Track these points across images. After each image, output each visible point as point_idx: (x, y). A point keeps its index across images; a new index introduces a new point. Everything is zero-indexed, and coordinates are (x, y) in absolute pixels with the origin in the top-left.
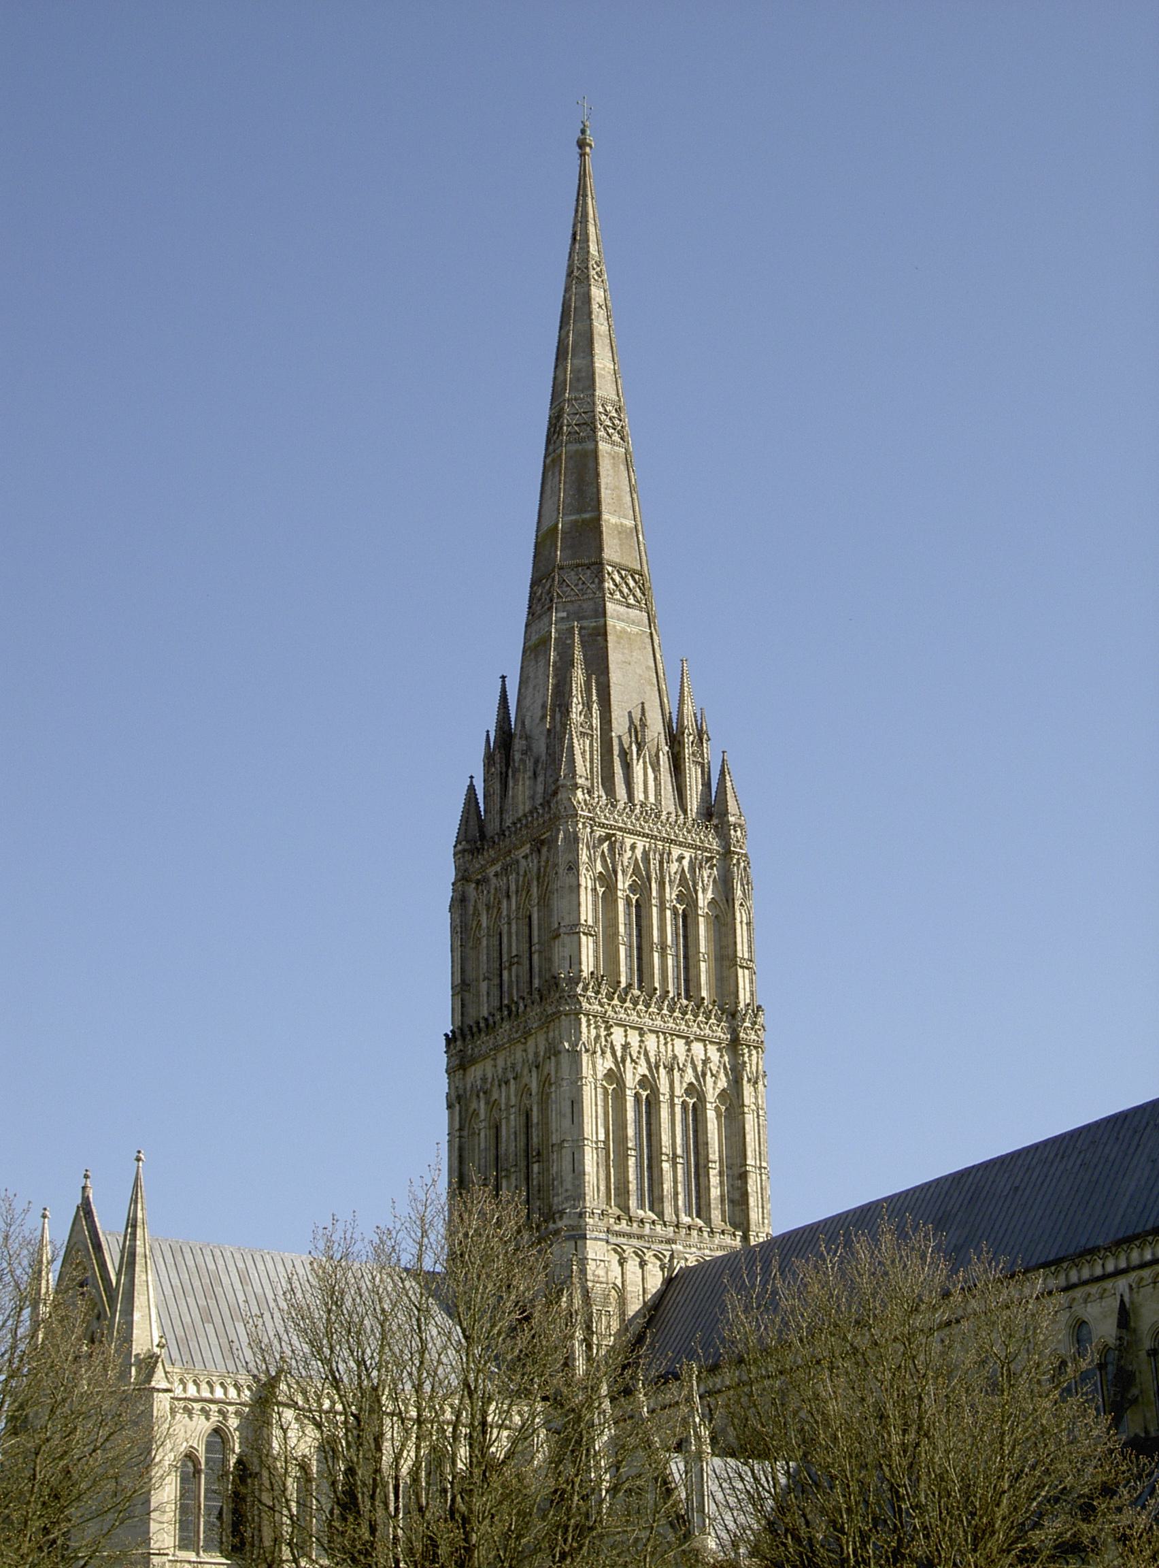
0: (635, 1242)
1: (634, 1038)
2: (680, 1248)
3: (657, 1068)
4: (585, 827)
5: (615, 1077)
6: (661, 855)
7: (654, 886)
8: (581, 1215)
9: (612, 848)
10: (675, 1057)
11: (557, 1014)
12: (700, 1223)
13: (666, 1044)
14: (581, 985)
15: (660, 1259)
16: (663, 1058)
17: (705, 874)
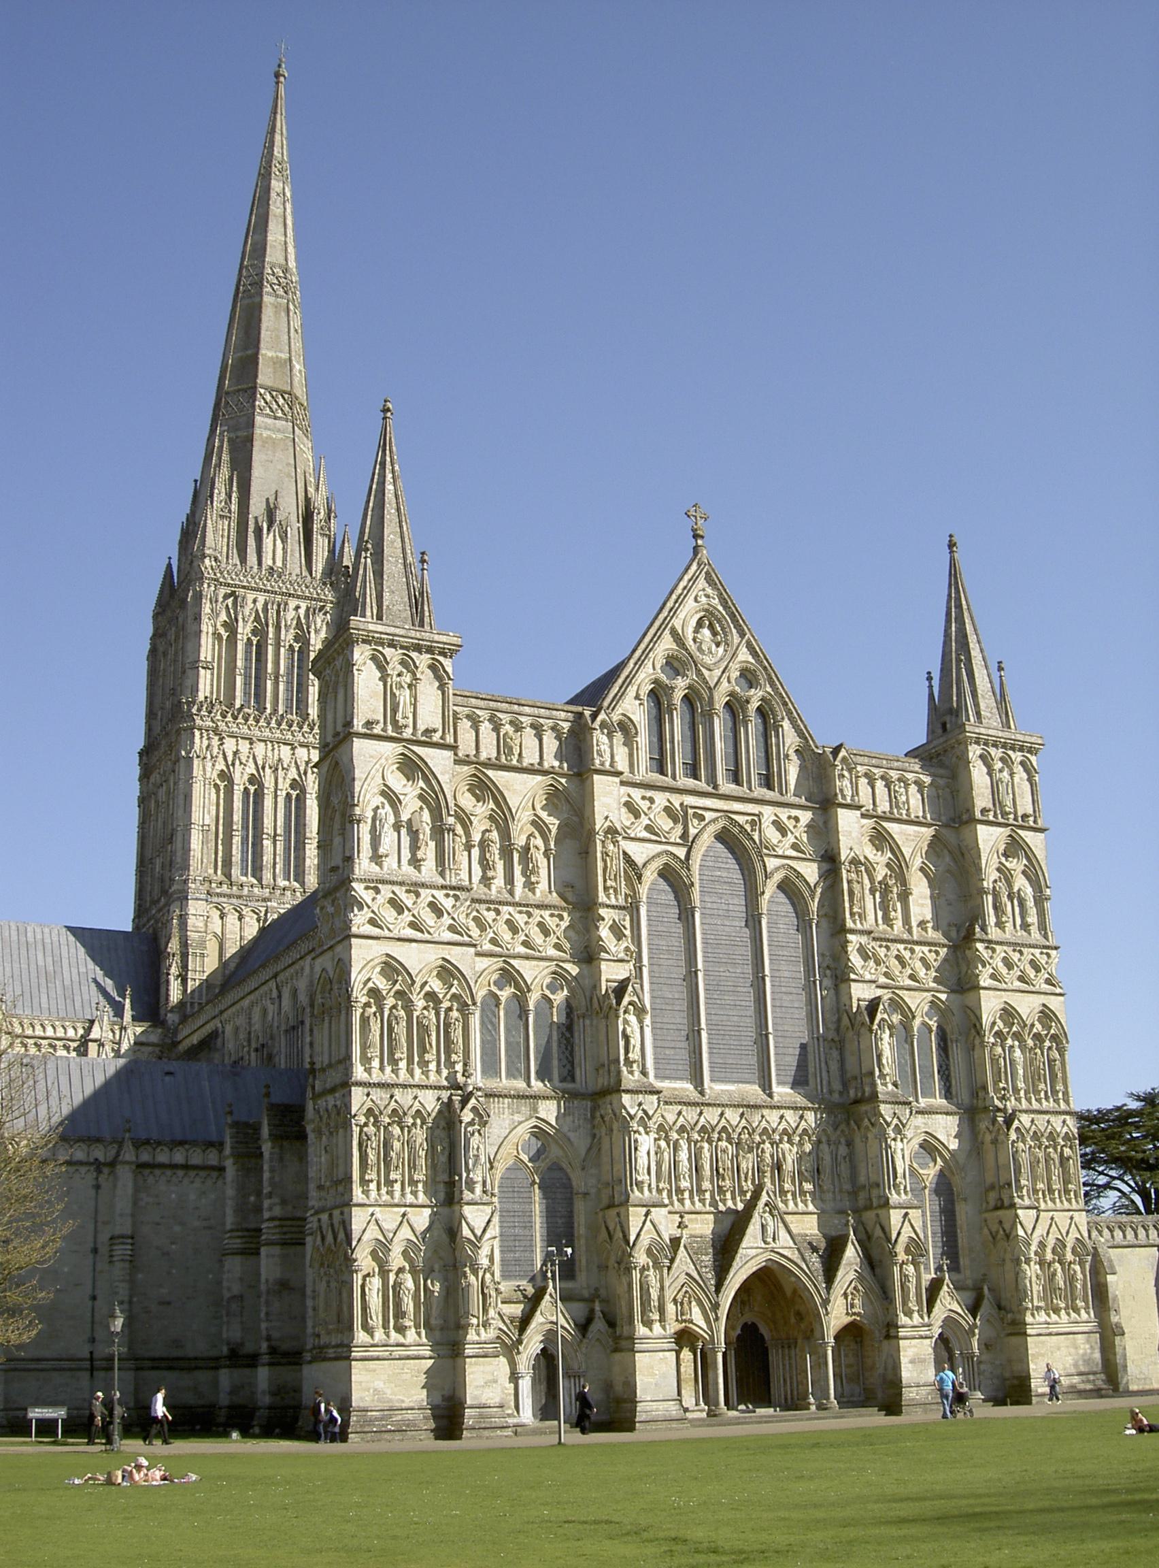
0: (234, 901)
1: (244, 746)
2: (275, 905)
3: (263, 768)
4: (209, 586)
5: (226, 776)
6: (279, 606)
7: (271, 629)
8: (186, 882)
9: (235, 603)
10: (280, 760)
11: (178, 732)
12: (296, 885)
13: (273, 750)
14: (196, 707)
15: (257, 914)
16: (270, 762)
17: (319, 620)
